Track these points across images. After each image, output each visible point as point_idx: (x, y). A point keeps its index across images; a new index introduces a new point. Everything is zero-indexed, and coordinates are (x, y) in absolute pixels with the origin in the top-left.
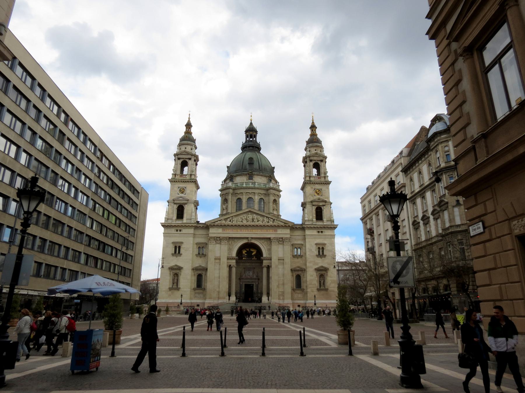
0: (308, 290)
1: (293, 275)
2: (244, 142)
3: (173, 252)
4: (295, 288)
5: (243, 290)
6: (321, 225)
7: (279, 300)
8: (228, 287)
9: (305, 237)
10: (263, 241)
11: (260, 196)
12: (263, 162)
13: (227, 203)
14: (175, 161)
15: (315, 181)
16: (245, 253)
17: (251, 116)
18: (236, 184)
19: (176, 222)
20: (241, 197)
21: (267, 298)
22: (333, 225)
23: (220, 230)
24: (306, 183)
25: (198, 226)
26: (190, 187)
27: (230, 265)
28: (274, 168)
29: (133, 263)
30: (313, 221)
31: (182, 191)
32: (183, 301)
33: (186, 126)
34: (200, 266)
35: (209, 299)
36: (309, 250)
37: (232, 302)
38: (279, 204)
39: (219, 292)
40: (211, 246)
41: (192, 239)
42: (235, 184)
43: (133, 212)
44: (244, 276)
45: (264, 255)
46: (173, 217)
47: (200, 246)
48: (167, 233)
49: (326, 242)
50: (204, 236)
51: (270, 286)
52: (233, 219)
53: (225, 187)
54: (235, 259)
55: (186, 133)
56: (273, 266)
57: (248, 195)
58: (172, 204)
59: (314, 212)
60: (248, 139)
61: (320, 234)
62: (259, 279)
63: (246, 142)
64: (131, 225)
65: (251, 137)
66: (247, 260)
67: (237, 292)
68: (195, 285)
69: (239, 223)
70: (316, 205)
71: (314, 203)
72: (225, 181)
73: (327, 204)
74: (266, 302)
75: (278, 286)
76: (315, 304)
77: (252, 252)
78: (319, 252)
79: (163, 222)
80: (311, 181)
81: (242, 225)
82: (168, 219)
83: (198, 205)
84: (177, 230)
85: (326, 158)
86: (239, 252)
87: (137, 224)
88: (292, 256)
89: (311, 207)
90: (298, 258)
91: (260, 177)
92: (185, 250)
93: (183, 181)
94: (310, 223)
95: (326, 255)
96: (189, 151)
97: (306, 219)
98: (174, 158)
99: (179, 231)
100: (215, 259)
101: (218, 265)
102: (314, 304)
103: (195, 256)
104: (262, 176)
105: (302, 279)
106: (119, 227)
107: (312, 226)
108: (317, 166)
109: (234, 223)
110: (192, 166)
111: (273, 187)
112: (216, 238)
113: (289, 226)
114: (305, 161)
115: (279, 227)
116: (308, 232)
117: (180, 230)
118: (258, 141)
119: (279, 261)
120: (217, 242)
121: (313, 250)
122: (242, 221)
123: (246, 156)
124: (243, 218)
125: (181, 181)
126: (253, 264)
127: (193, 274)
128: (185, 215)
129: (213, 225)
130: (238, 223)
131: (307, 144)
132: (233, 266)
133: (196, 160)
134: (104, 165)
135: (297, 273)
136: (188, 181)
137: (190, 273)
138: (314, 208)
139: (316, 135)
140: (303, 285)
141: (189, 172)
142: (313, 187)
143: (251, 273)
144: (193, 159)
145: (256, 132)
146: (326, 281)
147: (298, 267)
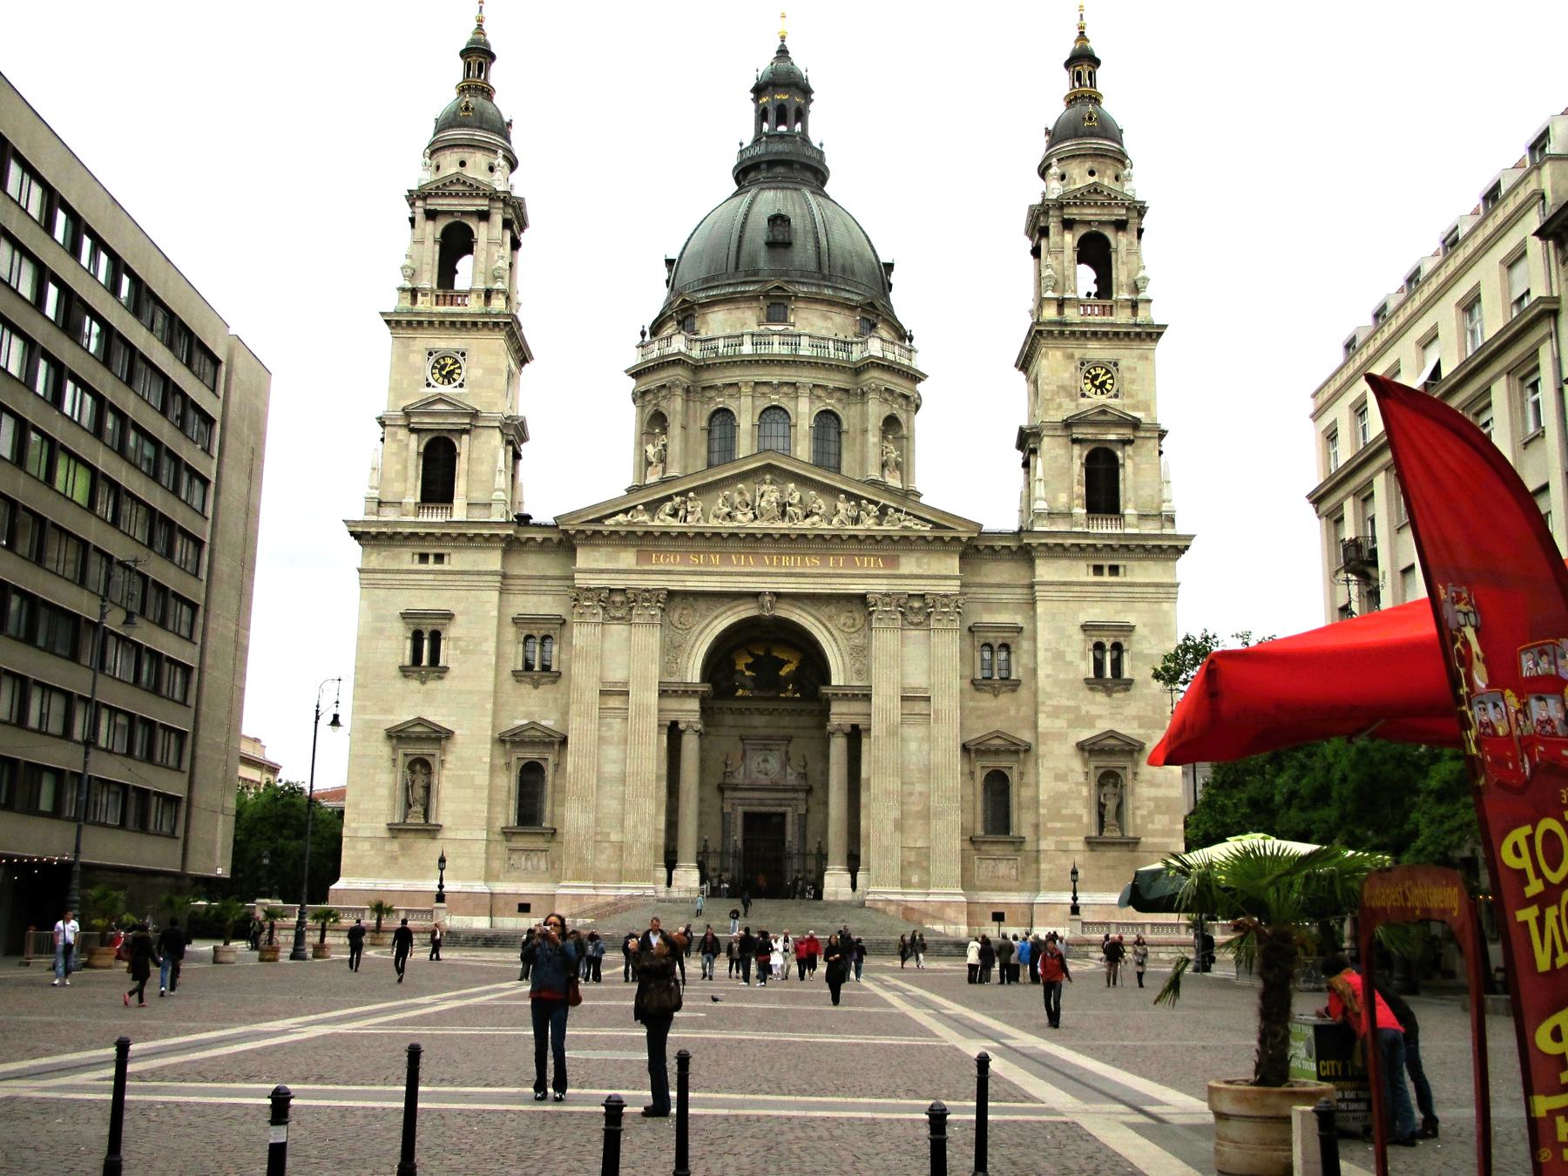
0: (1043, 845)
1: (972, 773)
2: (747, 143)
3: (408, 661)
4: (980, 832)
6: (1110, 536)
8: (662, 825)
10: (832, 610)
11: (819, 397)
12: (839, 238)
13: (664, 431)
14: (413, 226)
15: (1088, 324)
16: (748, 667)
17: (783, 17)
18: (710, 344)
19: (420, 519)
20: (732, 405)
21: (848, 877)
22: (1170, 537)
23: (627, 559)
24: (1040, 332)
26: (489, 351)
27: (674, 724)
28: (889, 267)
29: (191, 701)
30: (1070, 515)
31: (446, 368)
32: (449, 886)
33: (464, 54)
34: (533, 726)
36: (1049, 654)
37: (682, 895)
38: (909, 438)
39: (621, 851)
40: (586, 629)
41: (495, 595)
42: (701, 341)
43: (189, 453)
45: (837, 679)
46: (403, 495)
47: (535, 633)
48: (374, 571)
49: (1131, 619)
50: (549, 582)
51: (863, 823)
53: (654, 355)
54: (695, 692)
55: (462, 90)
56: (877, 728)
57: (764, 394)
58: (402, 434)
59: (1078, 469)
60: (766, 127)
61: (1106, 578)
62: (812, 789)
63: (757, 141)
64: (180, 515)
65: (781, 119)
67: (706, 846)
68: (507, 814)
71: (1079, 432)
73: (1142, 434)
74: (841, 898)
75: (900, 826)
76: (1075, 910)
77: (783, 663)
78: (1099, 666)
79: (359, 516)
80: (1066, 324)
81: (733, 535)
82: (380, 503)
83: (524, 439)
84: (424, 558)
85: (1141, 211)
86: (719, 660)
87: (209, 514)
89: (1062, 452)
91: (824, 308)
92: (464, 652)
93: (453, 324)
94: (1061, 526)
95: (1130, 682)
96: (480, 178)
98: (408, 212)
99: (431, 559)
101: (617, 723)
102: (1068, 909)
103: (509, 683)
104: (830, 302)
105: (1013, 790)
106: (115, 522)
107: (1068, 542)
108: (1095, 252)
110: (494, 248)
111: (884, 359)
112: (604, 595)
113: (958, 539)
114: (1037, 230)
115: (906, 542)
116: (1046, 571)
117: (439, 558)
118: (815, 137)
119: (908, 704)
120: (613, 613)
121: (1069, 658)
122: (729, 514)
123: (756, 208)
124: (737, 499)
125: (442, 323)
126: (786, 721)
128: (460, 486)
129: (595, 532)
130: (713, 522)
131: (1050, 146)
132: (689, 726)
133: (516, 222)
134: (18, 204)
136: (475, 324)
138: (1079, 454)
139: (1096, 99)
140: (1022, 822)
141: (481, 278)
142: (1078, 353)
143: (774, 764)
144: (497, 219)
145: (806, 91)
146: (1130, 803)
147: (998, 735)
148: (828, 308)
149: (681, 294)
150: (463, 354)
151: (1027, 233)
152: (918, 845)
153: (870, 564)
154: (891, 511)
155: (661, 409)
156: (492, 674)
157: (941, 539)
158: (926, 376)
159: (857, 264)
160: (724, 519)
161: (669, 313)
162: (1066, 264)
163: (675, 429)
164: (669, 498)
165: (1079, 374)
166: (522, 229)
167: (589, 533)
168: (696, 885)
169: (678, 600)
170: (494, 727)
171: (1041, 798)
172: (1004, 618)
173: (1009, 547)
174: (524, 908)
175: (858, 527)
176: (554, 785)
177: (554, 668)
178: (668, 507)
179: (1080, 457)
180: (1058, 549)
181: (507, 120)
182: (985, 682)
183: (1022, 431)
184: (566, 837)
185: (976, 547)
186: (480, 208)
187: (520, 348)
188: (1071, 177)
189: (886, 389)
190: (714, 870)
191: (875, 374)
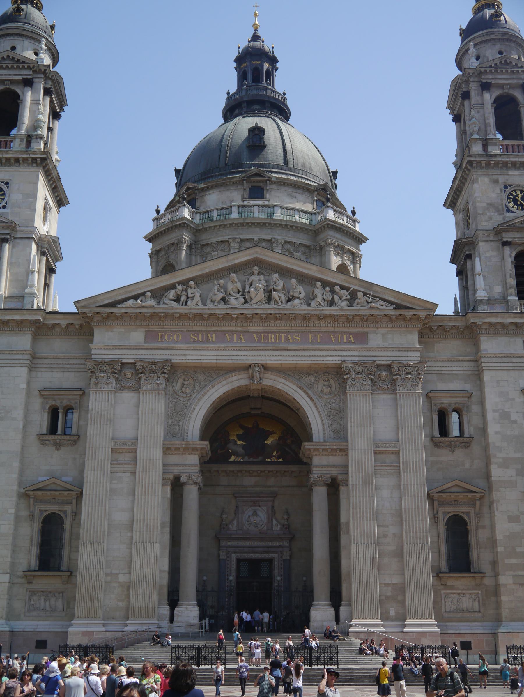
0: (502, 580)
1: (434, 518)
7: (382, 620)
8: (166, 567)
9: (478, 367)
17: (256, 15)
21: (332, 611)
24: (470, 163)
25: (51, 322)
28: (335, 173)
35: (85, 617)
36: (497, 414)
37: (183, 630)
41: (24, 371)
42: (200, 213)
44: (235, 528)
47: (58, 404)
50: (71, 362)
52: (190, 291)
53: (166, 222)
54: (194, 449)
70: (516, 244)
71: (508, 237)
77: (267, 435)
81: (226, 317)
83: (58, 258)
88: (428, 439)
89: (494, 253)
90: (452, 448)
91: (290, 190)
97: (481, 294)
100: (113, 451)
113: (418, 318)
121: (514, 417)
122: (223, 299)
123: (239, 127)
124: (230, 287)
127: (24, 513)
129: (109, 316)
131: (463, 41)
135: (452, 510)
136: (17, 160)
137: (13, 511)
138: (509, 254)
142: (501, 179)
143: (262, 516)
145: (273, 61)
148: (294, 190)
149: (185, 184)
150: (7, 184)
151: (449, 107)
152: (395, 581)
154: (360, 295)
155: (171, 261)
156: (20, 436)
157: (403, 318)
158: (367, 239)
159: (313, 164)
160: (219, 303)
161: (177, 198)
162: (486, 115)
164: (173, 287)
165: (503, 194)
166: (62, 109)
167: (105, 315)
168: (196, 621)
170: (20, 484)
171: (498, 538)
172: (455, 385)
173: (457, 327)
174: (41, 645)
175: (332, 307)
176: (71, 534)
177: (74, 431)
178: (172, 294)
179: (511, 255)
180: (499, 327)
181: (50, 23)
182: (443, 439)
183: (457, 244)
184: (79, 578)
185: (430, 329)
186: (25, 77)
187: (56, 187)
188: (485, 56)
189: (338, 245)
190: (212, 607)
191: (331, 233)
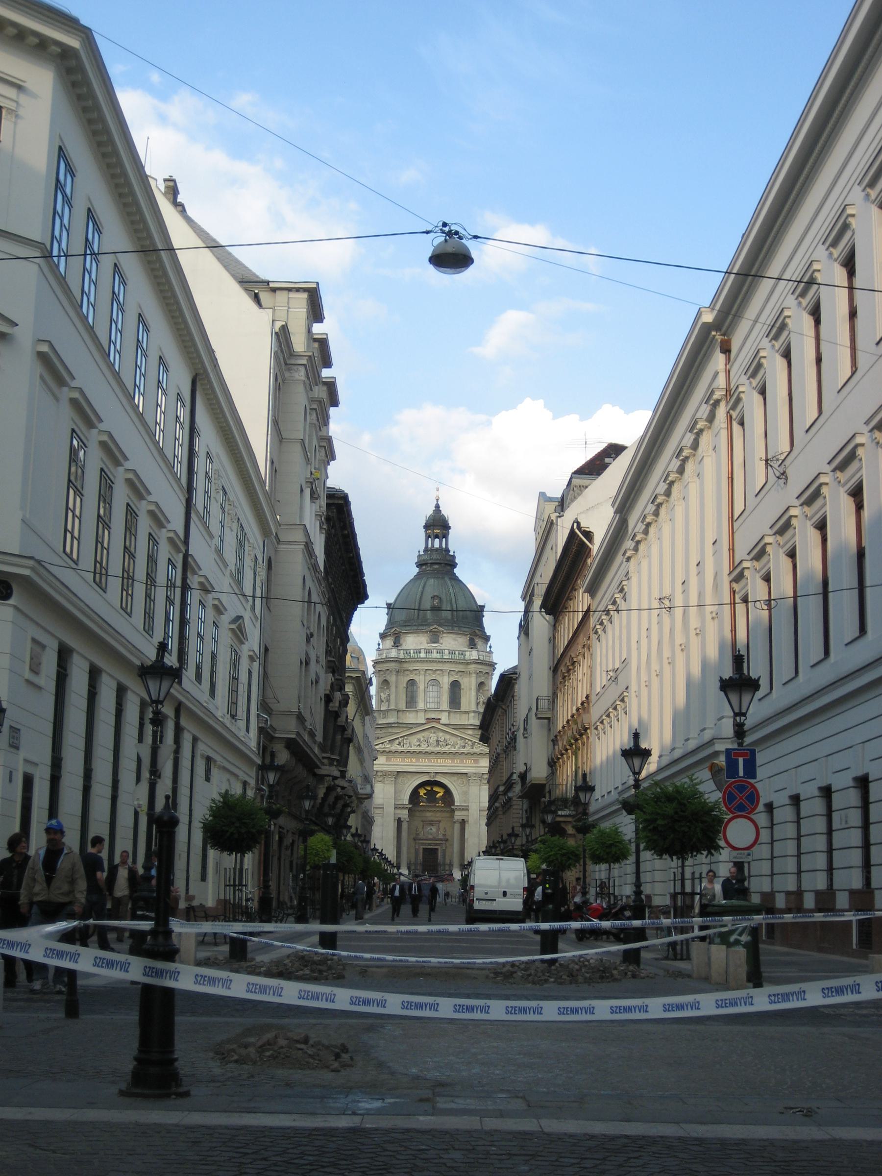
5: (421, 858)
16: (424, 794)
17: (438, 490)
20: (416, 678)
27: (399, 819)
63: (426, 550)
65: (437, 536)
66: (428, 806)
69: (414, 748)
72: (383, 636)
86: (415, 793)
109: (406, 748)
111: (479, 659)
118: (451, 547)
126: (439, 814)
145: (449, 528)
153: (469, 762)
163: (393, 689)
164: (398, 738)
169: (401, 774)
178: (397, 742)
